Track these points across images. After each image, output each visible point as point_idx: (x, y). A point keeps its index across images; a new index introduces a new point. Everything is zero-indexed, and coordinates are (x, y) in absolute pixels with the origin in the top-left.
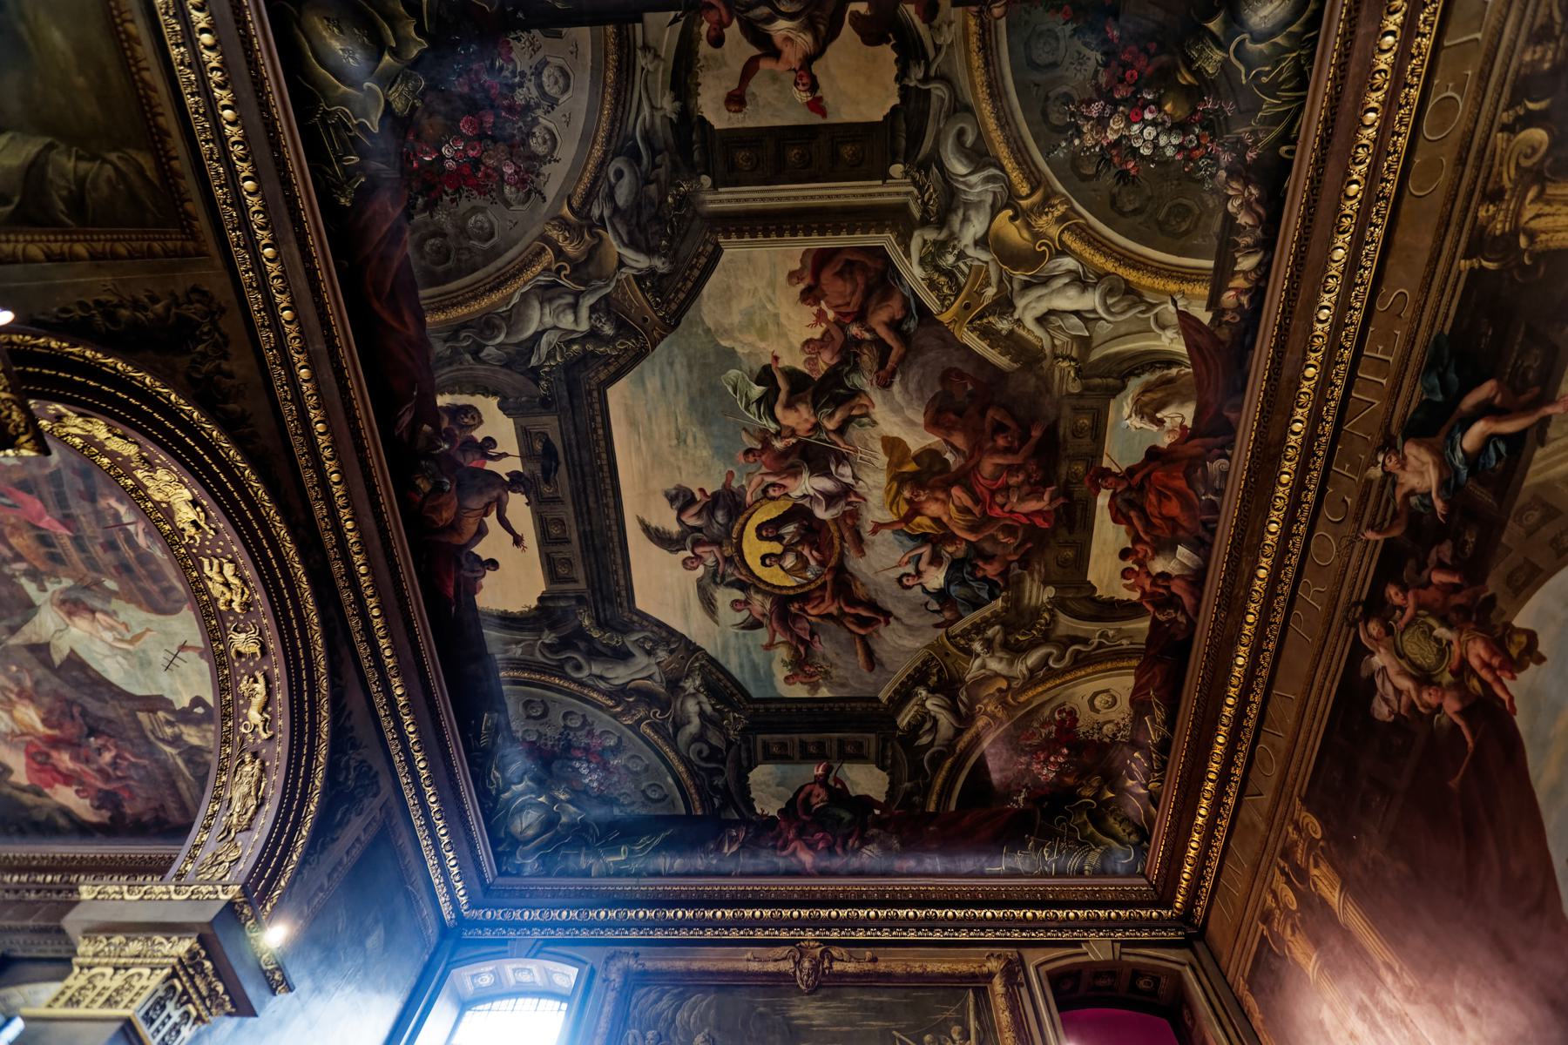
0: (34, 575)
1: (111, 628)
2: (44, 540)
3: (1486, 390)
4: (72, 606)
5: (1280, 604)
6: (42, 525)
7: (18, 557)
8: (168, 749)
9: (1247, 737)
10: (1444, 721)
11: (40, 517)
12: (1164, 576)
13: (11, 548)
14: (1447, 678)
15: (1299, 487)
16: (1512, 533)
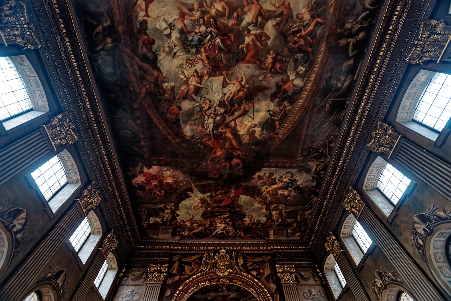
0: (211, 196)
1: (198, 206)
2: (220, 201)
4: (203, 201)
7: (216, 195)
8: (163, 206)
11: (225, 202)
13: (219, 194)
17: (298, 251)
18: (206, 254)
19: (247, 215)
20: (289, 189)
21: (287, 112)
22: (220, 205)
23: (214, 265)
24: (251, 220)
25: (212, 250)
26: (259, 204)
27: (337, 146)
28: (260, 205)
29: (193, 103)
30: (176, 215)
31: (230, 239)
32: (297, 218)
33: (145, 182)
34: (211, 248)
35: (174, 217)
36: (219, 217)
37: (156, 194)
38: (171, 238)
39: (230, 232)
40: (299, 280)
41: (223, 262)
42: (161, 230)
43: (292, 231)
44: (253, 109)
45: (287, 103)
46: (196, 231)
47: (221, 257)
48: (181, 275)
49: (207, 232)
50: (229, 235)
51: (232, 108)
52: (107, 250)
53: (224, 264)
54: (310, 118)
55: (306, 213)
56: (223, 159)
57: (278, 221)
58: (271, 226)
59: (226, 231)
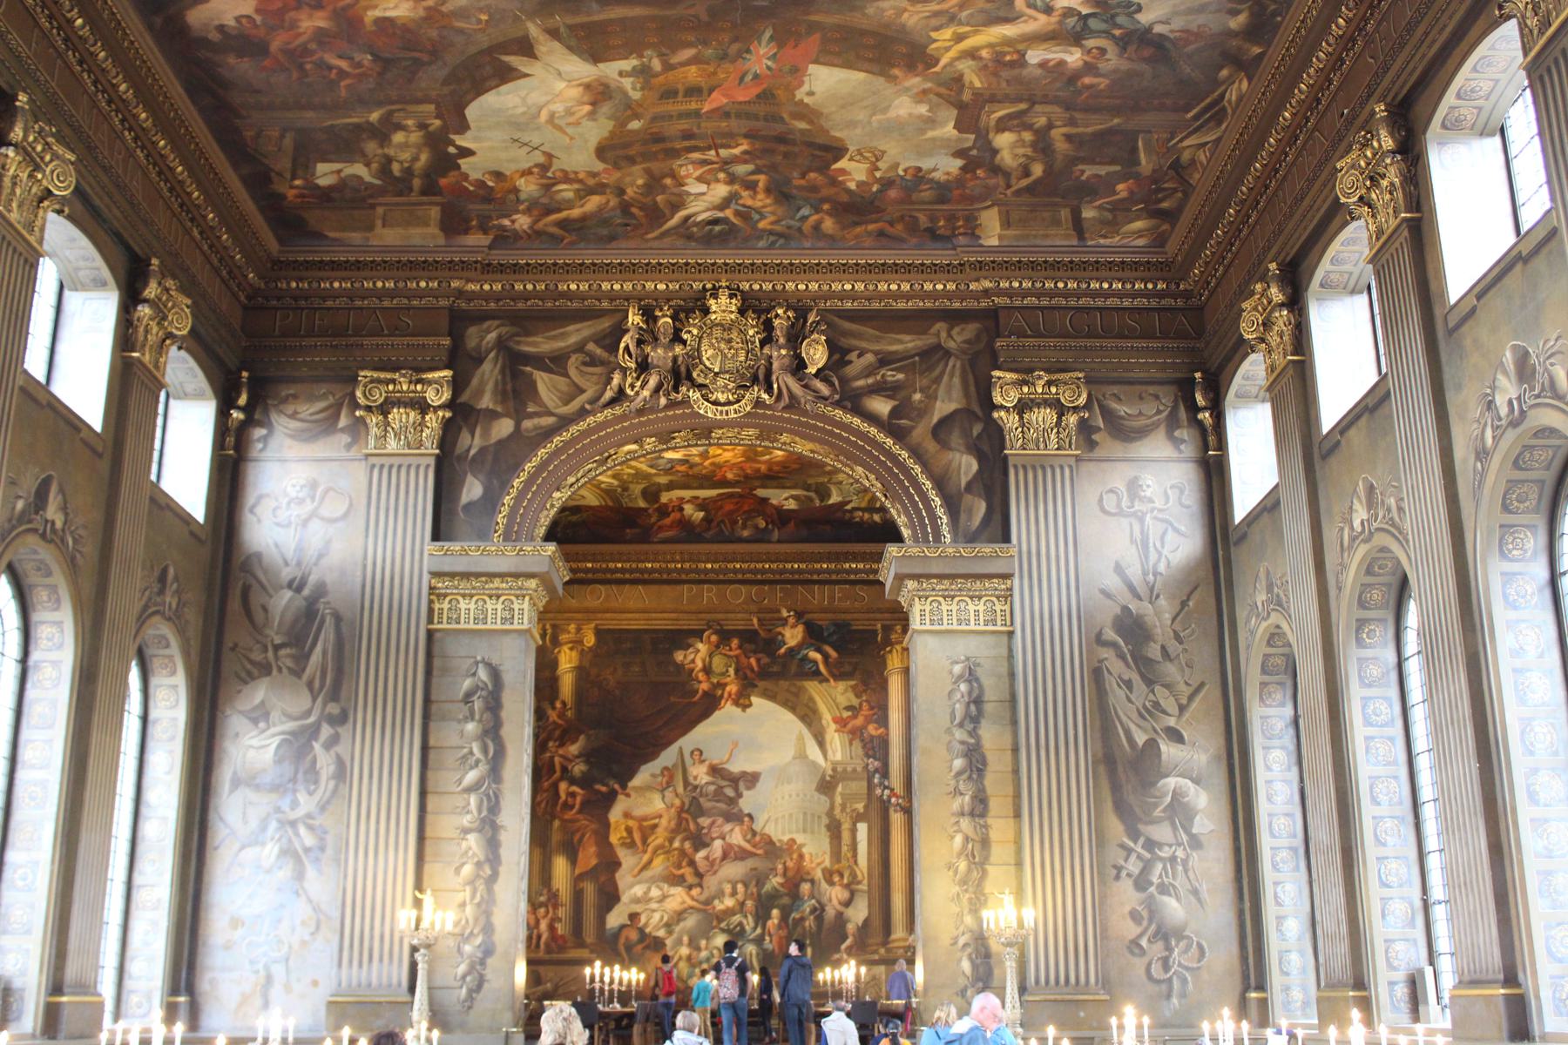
1: (569, 112)
3: (833, 654)
4: (599, 94)
5: (693, 576)
6: (714, 95)
7: (668, 67)
8: (375, 116)
9: (600, 576)
10: (696, 686)
12: (682, 509)
14: (715, 681)
15: (763, 571)
16: (784, 684)
17: (1127, 303)
18: (634, 318)
19: (852, 148)
20: (1091, 43)
22: (694, 106)
23: (680, 376)
24: (877, 169)
25: (668, 297)
26: (920, 102)
28: (923, 109)
30: (452, 150)
31: (761, 244)
32: (1139, 164)
33: (258, 19)
34: (661, 287)
35: (445, 160)
36: (696, 156)
37: (330, 68)
38: (441, 241)
39: (763, 217)
40: (1096, 437)
41: (724, 356)
42: (380, 210)
43: (1109, 216)
46: (575, 213)
47: (717, 332)
48: (519, 415)
49: (633, 216)
50: (754, 227)
52: (161, 348)
53: (729, 365)
55: (1187, 143)
57: (1026, 173)
58: (986, 195)
59: (737, 213)
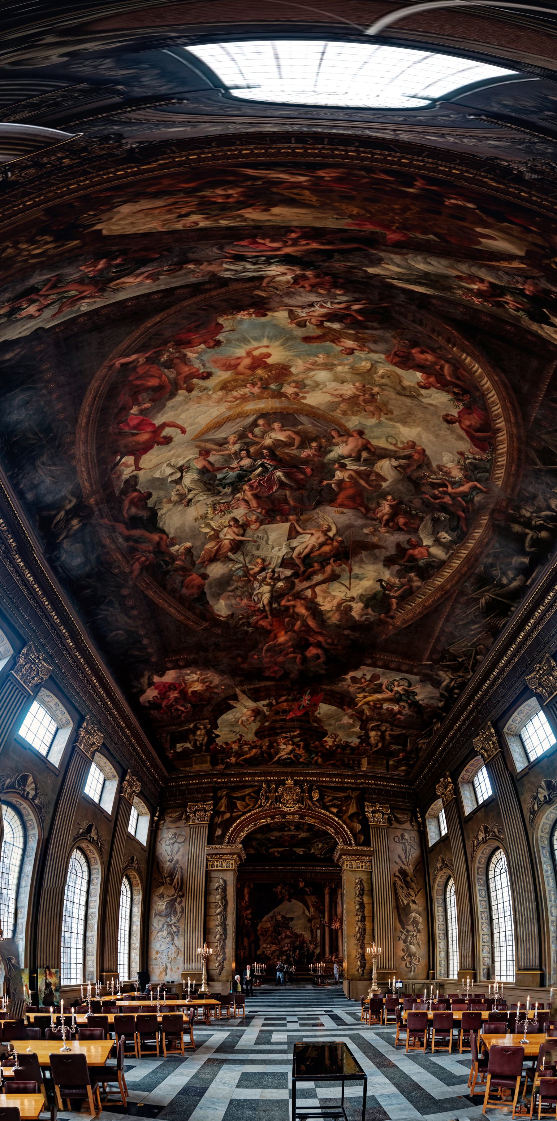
21: (414, 589)
27: (486, 661)
29: (230, 566)
44: (350, 572)
45: (415, 576)
51: (307, 569)
54: (453, 608)
56: (289, 647)
